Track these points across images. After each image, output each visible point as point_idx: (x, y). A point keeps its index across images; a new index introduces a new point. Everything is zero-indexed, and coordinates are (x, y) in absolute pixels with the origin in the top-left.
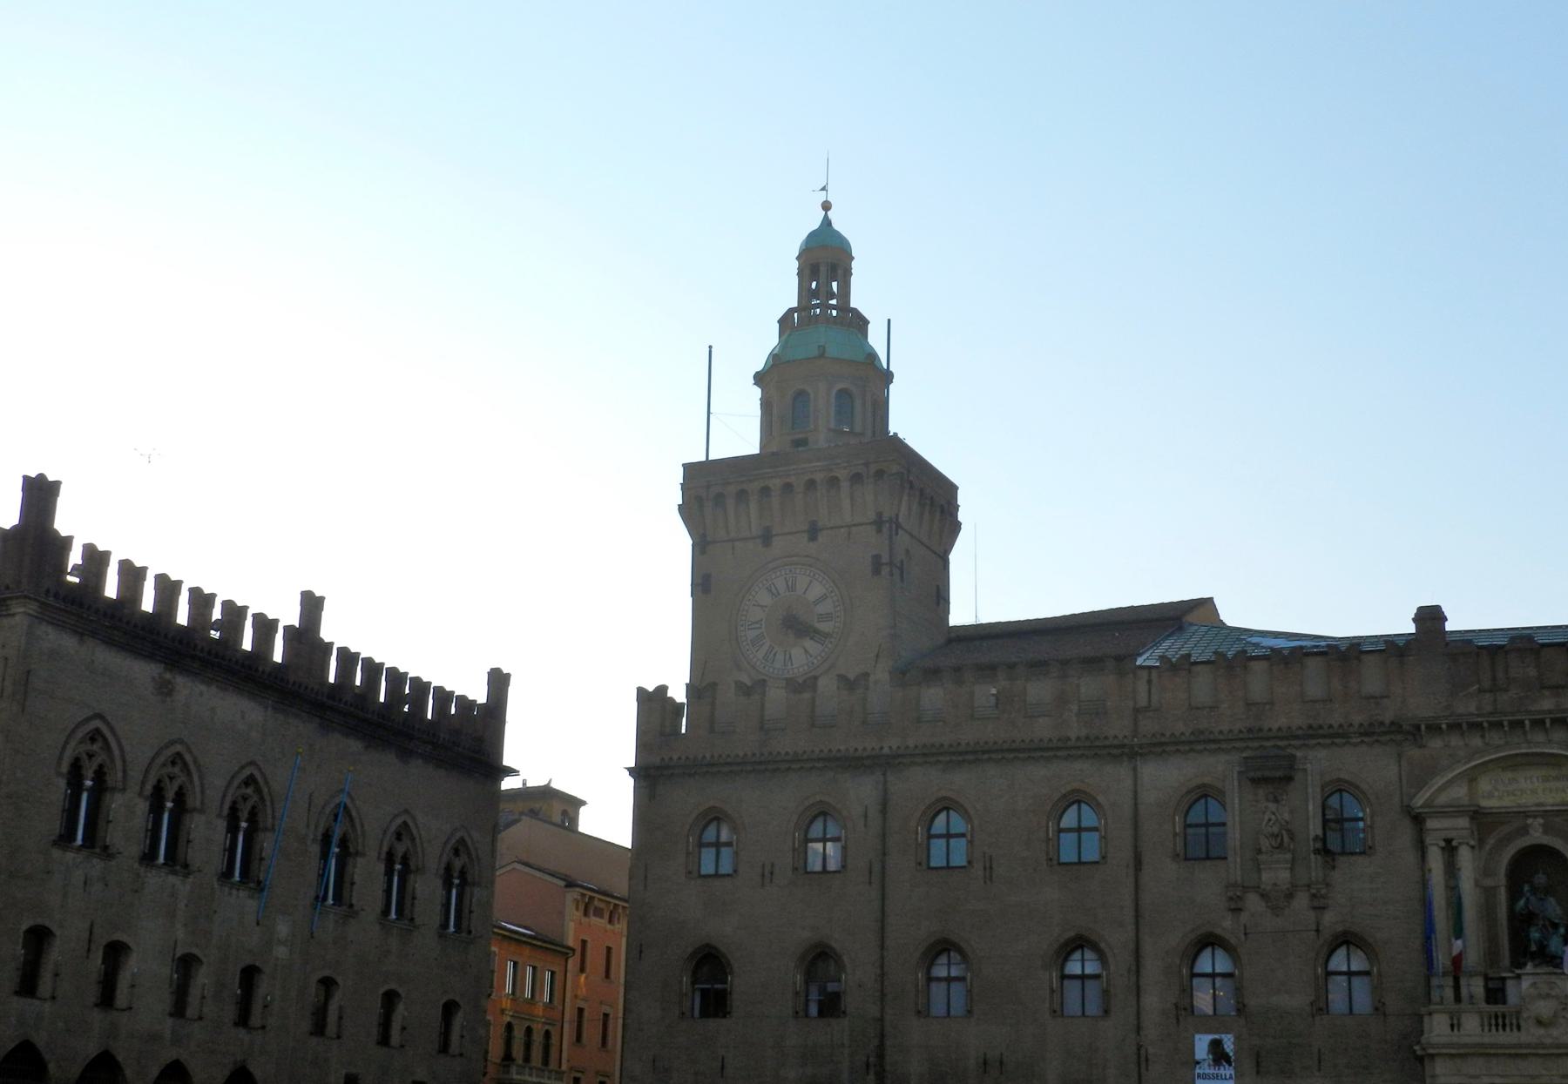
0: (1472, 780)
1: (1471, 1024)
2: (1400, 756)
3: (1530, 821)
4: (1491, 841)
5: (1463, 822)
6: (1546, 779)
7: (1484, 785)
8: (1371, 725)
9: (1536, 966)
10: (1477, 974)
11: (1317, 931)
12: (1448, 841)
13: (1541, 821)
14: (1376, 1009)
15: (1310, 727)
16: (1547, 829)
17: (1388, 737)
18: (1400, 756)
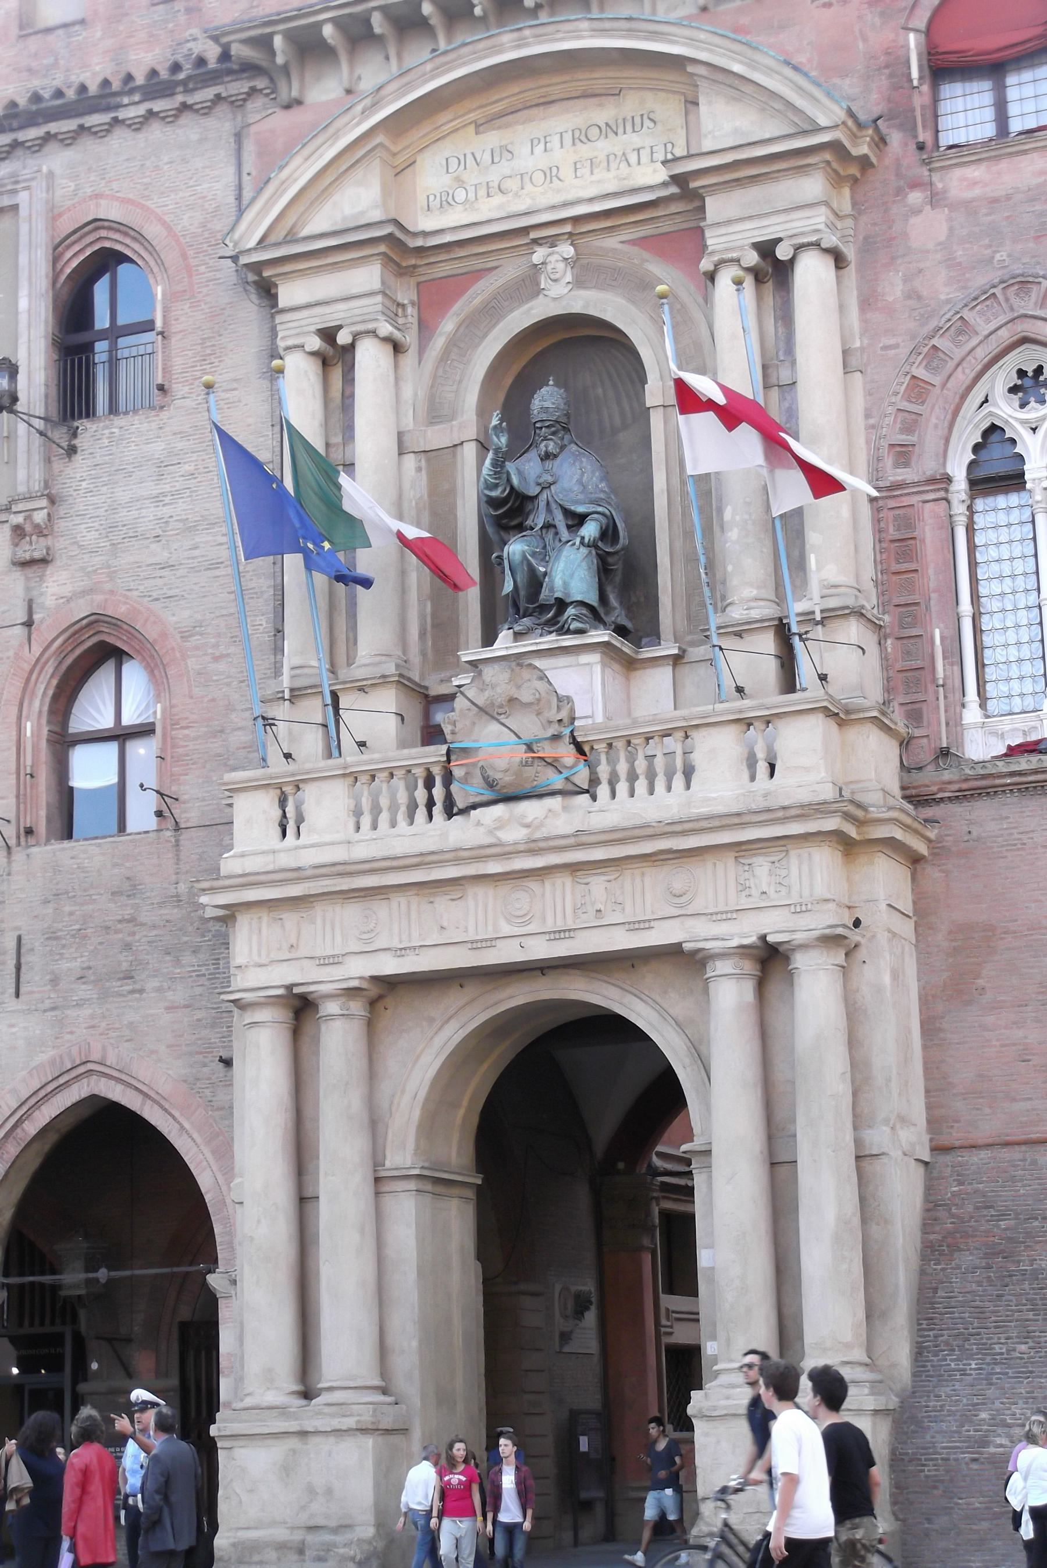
0: (401, 170)
1: (327, 809)
2: (238, 137)
3: (539, 255)
4: (448, 326)
5: (368, 276)
6: (581, 137)
7: (431, 175)
8: (176, 67)
9: (518, 636)
10: (384, 681)
11: (29, 624)
12: (328, 335)
13: (567, 250)
14: (159, 814)
15: (36, 98)
16: (584, 272)
17: (208, 94)
18: (238, 137)
